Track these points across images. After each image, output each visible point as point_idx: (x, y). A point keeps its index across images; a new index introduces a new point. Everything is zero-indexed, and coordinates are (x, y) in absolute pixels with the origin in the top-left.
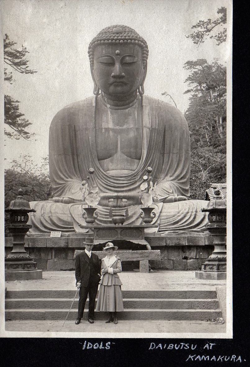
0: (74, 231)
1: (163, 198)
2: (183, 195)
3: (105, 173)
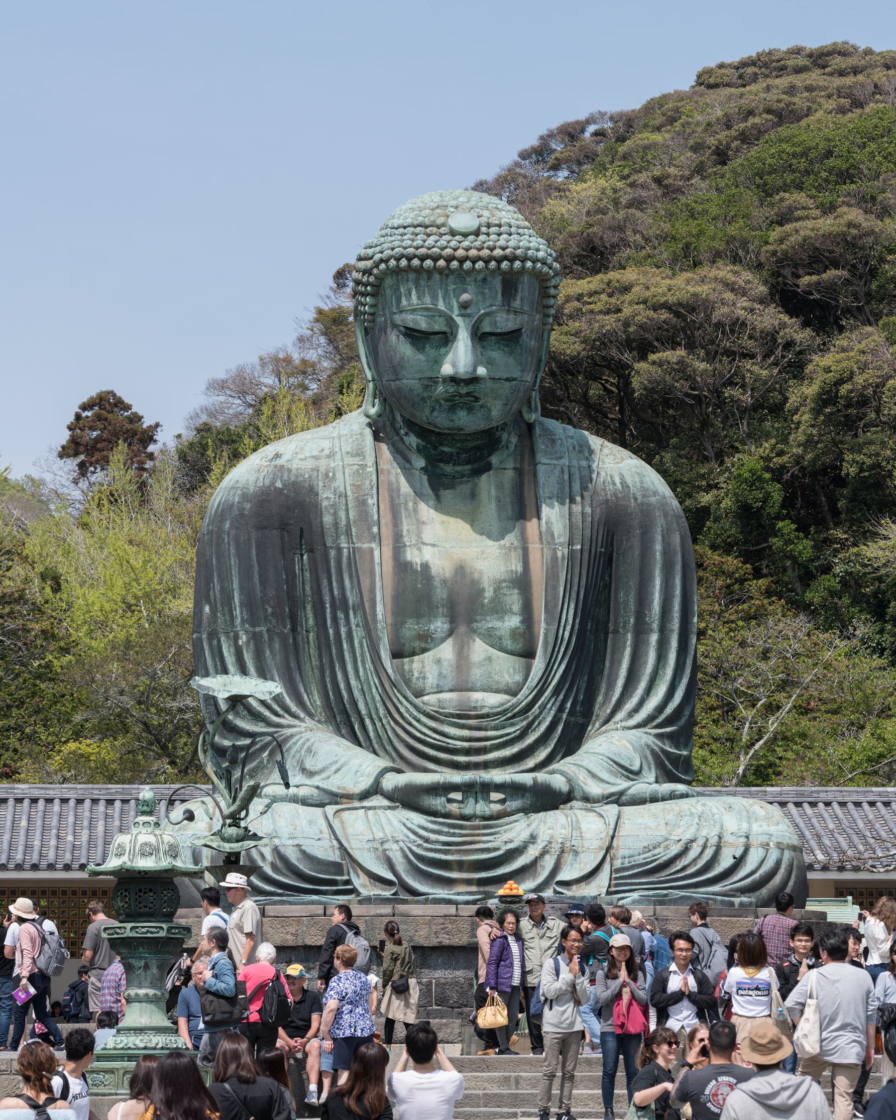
0: (354, 891)
3: (417, 701)
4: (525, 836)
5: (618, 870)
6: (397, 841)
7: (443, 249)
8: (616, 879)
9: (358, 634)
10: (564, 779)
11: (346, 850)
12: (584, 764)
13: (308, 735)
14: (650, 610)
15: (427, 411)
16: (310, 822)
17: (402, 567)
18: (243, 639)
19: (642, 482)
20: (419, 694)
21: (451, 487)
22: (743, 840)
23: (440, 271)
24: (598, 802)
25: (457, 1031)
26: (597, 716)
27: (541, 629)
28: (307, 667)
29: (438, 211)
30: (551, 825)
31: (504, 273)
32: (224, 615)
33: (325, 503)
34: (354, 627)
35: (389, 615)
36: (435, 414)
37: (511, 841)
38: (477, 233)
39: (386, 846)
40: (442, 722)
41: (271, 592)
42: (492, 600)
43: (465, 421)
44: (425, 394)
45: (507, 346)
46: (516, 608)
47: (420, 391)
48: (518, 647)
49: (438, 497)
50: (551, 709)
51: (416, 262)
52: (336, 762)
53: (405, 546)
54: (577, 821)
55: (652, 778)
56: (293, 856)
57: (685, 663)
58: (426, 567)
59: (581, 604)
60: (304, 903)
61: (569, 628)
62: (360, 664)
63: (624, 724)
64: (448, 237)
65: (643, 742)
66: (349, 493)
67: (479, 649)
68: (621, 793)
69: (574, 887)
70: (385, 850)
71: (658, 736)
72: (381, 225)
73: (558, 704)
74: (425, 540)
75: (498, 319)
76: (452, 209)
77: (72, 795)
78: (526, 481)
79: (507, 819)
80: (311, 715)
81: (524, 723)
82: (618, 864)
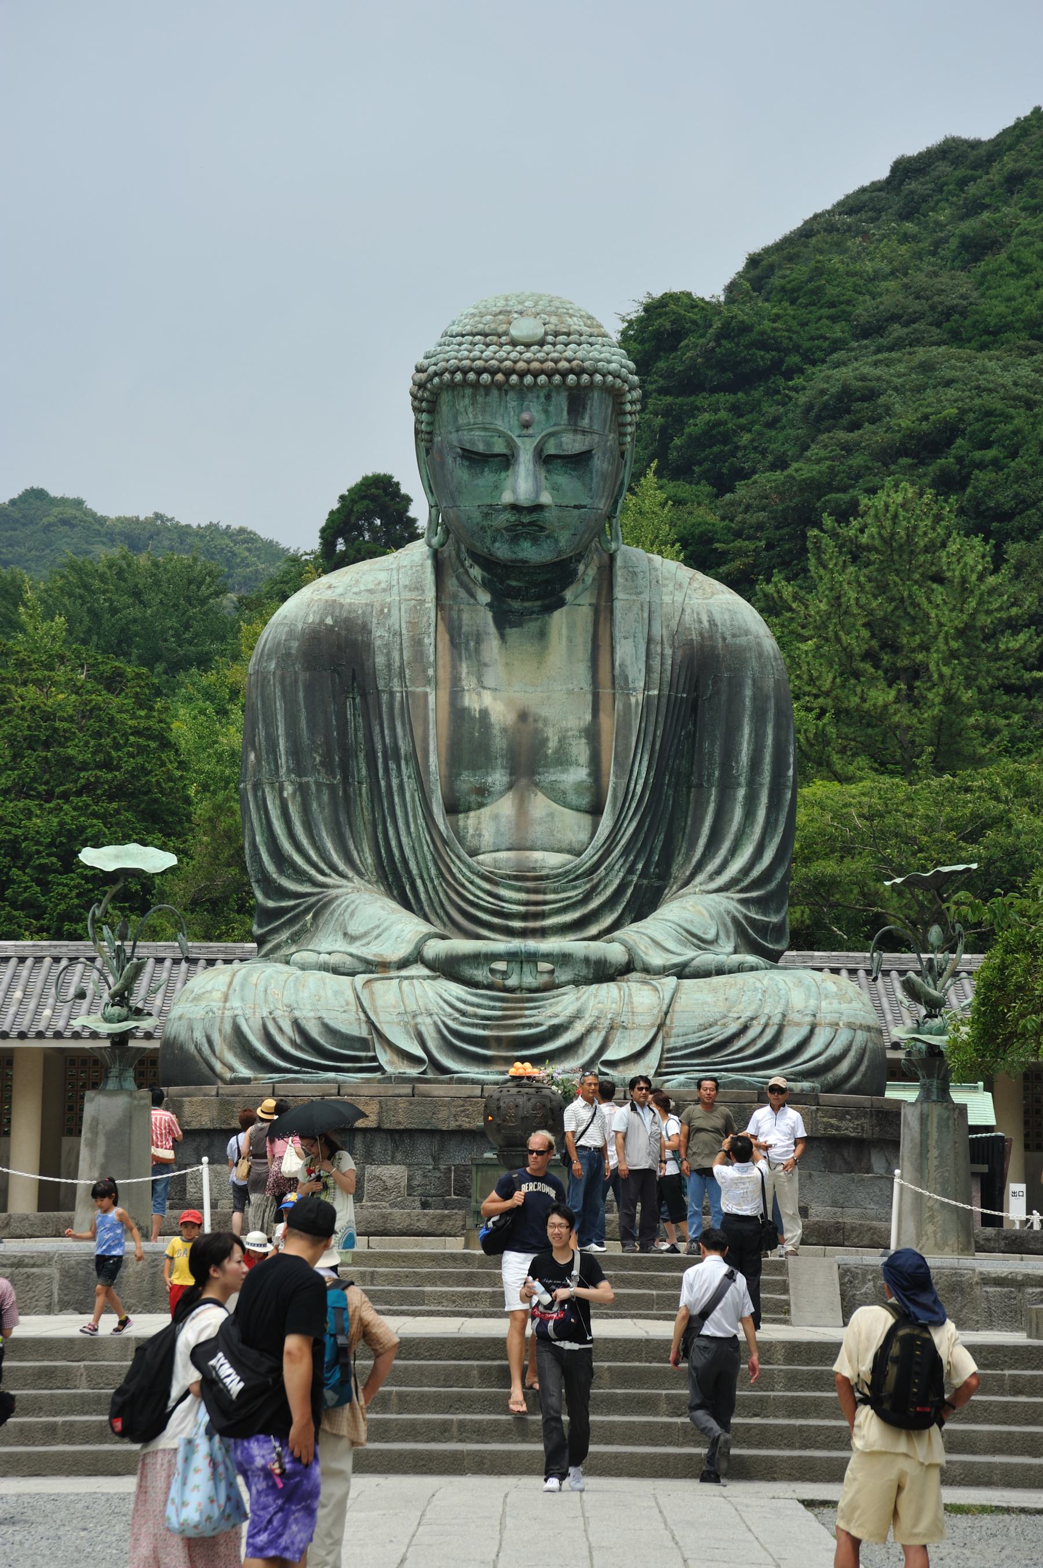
0: (380, 1069)
1: (677, 960)
2: (756, 949)
3: (470, 860)
4: (570, 1010)
5: (670, 1050)
6: (431, 1015)
7: (501, 361)
8: (668, 1059)
9: (410, 786)
10: (622, 948)
11: (373, 1024)
12: (648, 932)
13: (353, 896)
14: (737, 762)
15: (488, 541)
16: (336, 993)
17: (458, 714)
18: (289, 790)
19: (732, 620)
20: (473, 853)
21: (519, 624)
22: (809, 1019)
23: (499, 386)
24: (659, 974)
25: (460, 1223)
26: (676, 878)
27: (611, 781)
28: (359, 822)
29: (501, 317)
30: (602, 998)
31: (570, 389)
32: (269, 764)
33: (378, 643)
34: (405, 779)
35: (443, 766)
36: (497, 545)
37: (557, 1016)
38: (542, 343)
39: (419, 1020)
40: (496, 884)
41: (320, 740)
42: (557, 751)
43: (530, 552)
44: (485, 523)
45: (575, 470)
47: (479, 519)
48: (585, 801)
49: (502, 637)
51: (471, 376)
52: (378, 926)
53: (463, 690)
54: (630, 995)
55: (730, 948)
56: (315, 1032)
57: (777, 820)
58: (484, 713)
60: (318, 1082)
61: (641, 781)
62: (411, 820)
63: (703, 887)
64: (508, 348)
65: (722, 909)
66: (404, 632)
67: (540, 805)
68: (685, 965)
69: (621, 1068)
70: (417, 1024)
71: (742, 901)
72: (442, 332)
73: (627, 865)
74: (486, 684)
75: (564, 439)
76: (516, 315)
77: (169, 954)
78: (602, 619)
79: (555, 992)
80: (360, 874)
81: (588, 886)
82: (672, 1042)
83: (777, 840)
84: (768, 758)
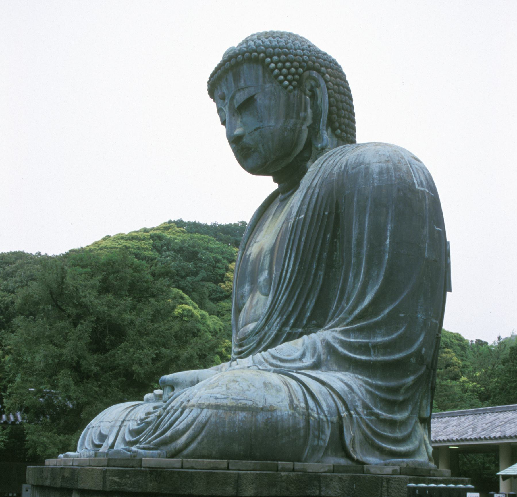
46: (267, 266)
50: (276, 327)
57: (378, 275)
58: (250, 255)
59: (301, 252)
61: (290, 270)
83: (377, 287)
84: (366, 236)
